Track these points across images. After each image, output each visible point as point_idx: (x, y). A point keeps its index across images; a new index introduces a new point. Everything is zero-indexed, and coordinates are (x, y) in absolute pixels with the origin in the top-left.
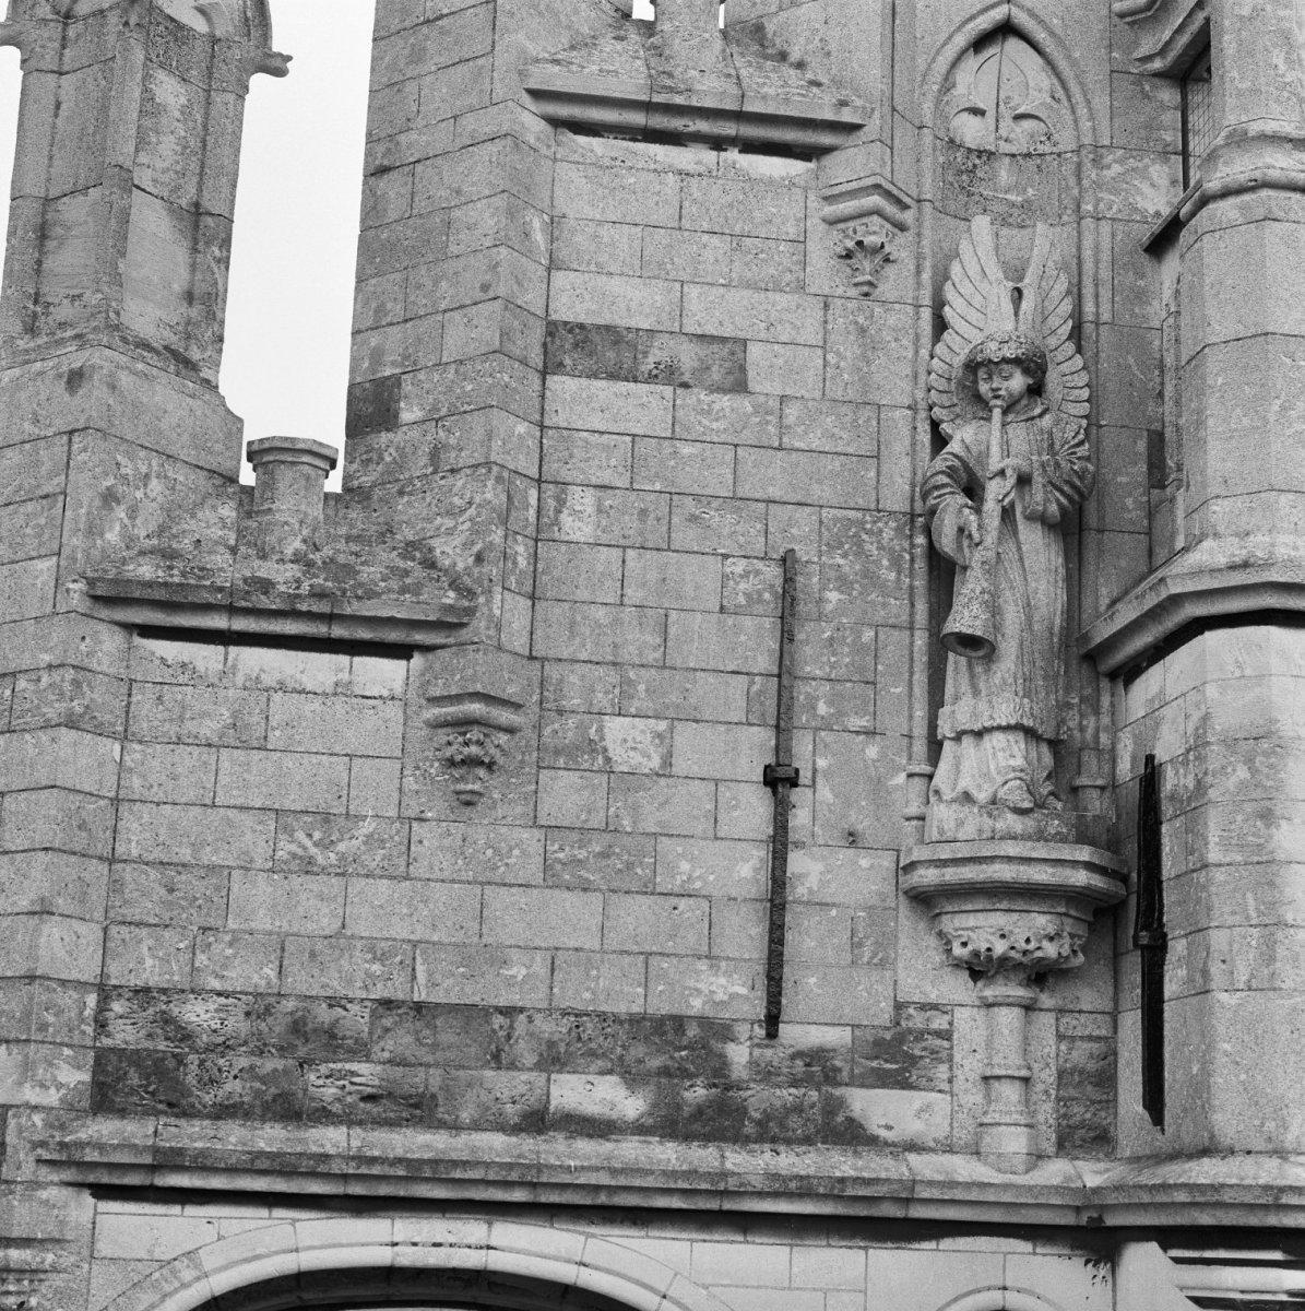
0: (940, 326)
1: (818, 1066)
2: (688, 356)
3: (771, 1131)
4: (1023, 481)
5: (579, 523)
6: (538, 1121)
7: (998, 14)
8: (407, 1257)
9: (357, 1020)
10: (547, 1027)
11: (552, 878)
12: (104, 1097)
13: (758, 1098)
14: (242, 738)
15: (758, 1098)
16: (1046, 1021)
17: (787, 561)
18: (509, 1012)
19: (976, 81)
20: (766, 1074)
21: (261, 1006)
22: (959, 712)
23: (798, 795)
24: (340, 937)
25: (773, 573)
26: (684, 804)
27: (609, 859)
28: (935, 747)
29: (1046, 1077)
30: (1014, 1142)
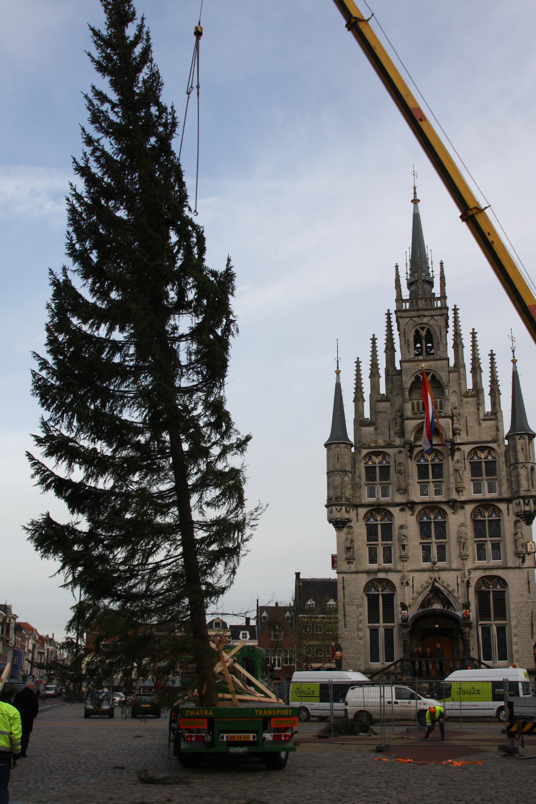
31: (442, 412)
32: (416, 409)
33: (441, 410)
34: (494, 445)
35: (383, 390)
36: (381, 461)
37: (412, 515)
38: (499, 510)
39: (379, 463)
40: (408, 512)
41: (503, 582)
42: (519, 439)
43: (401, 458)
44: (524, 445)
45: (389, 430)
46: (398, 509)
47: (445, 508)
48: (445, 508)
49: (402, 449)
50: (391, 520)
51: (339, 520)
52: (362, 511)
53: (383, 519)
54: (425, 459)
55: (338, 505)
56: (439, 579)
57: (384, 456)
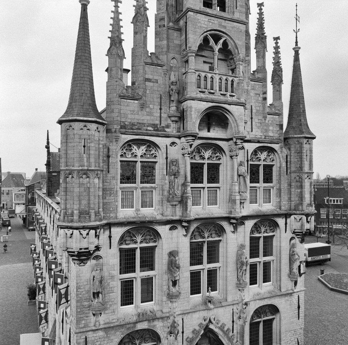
0: (170, 79)
1: (163, 127)
2: (154, 81)
3: (160, 131)
4: (176, 90)
5: (148, 92)
6: (147, 130)
7: (173, 57)
8: (140, 138)
9: (136, 124)
10: (147, 124)
11: (147, 115)
12: (121, 128)
13: (160, 129)
14: (128, 106)
15: (160, 129)
16: (176, 125)
17: (161, 95)
18: (145, 123)
19: (172, 62)
20: (160, 127)
21: (130, 123)
22: (171, 105)
23: (162, 110)
24: (135, 118)
25: (160, 96)
26: (155, 111)
27: (150, 114)
28: (170, 108)
29: (176, 128)
30: (175, 132)
31: (234, 96)
32: (202, 86)
33: (234, 94)
34: (276, 147)
35: (151, 48)
36: (145, 154)
37: (186, 236)
38: (276, 225)
39: (142, 156)
40: (180, 231)
41: (274, 310)
42: (306, 143)
43: (175, 153)
44: (308, 152)
45: (161, 109)
46: (168, 227)
47: (225, 224)
48: (225, 224)
49: (176, 140)
50: (155, 242)
51: (83, 250)
52: (118, 232)
53: (145, 239)
54: (201, 156)
55: (84, 228)
56: (214, 319)
57: (149, 146)
